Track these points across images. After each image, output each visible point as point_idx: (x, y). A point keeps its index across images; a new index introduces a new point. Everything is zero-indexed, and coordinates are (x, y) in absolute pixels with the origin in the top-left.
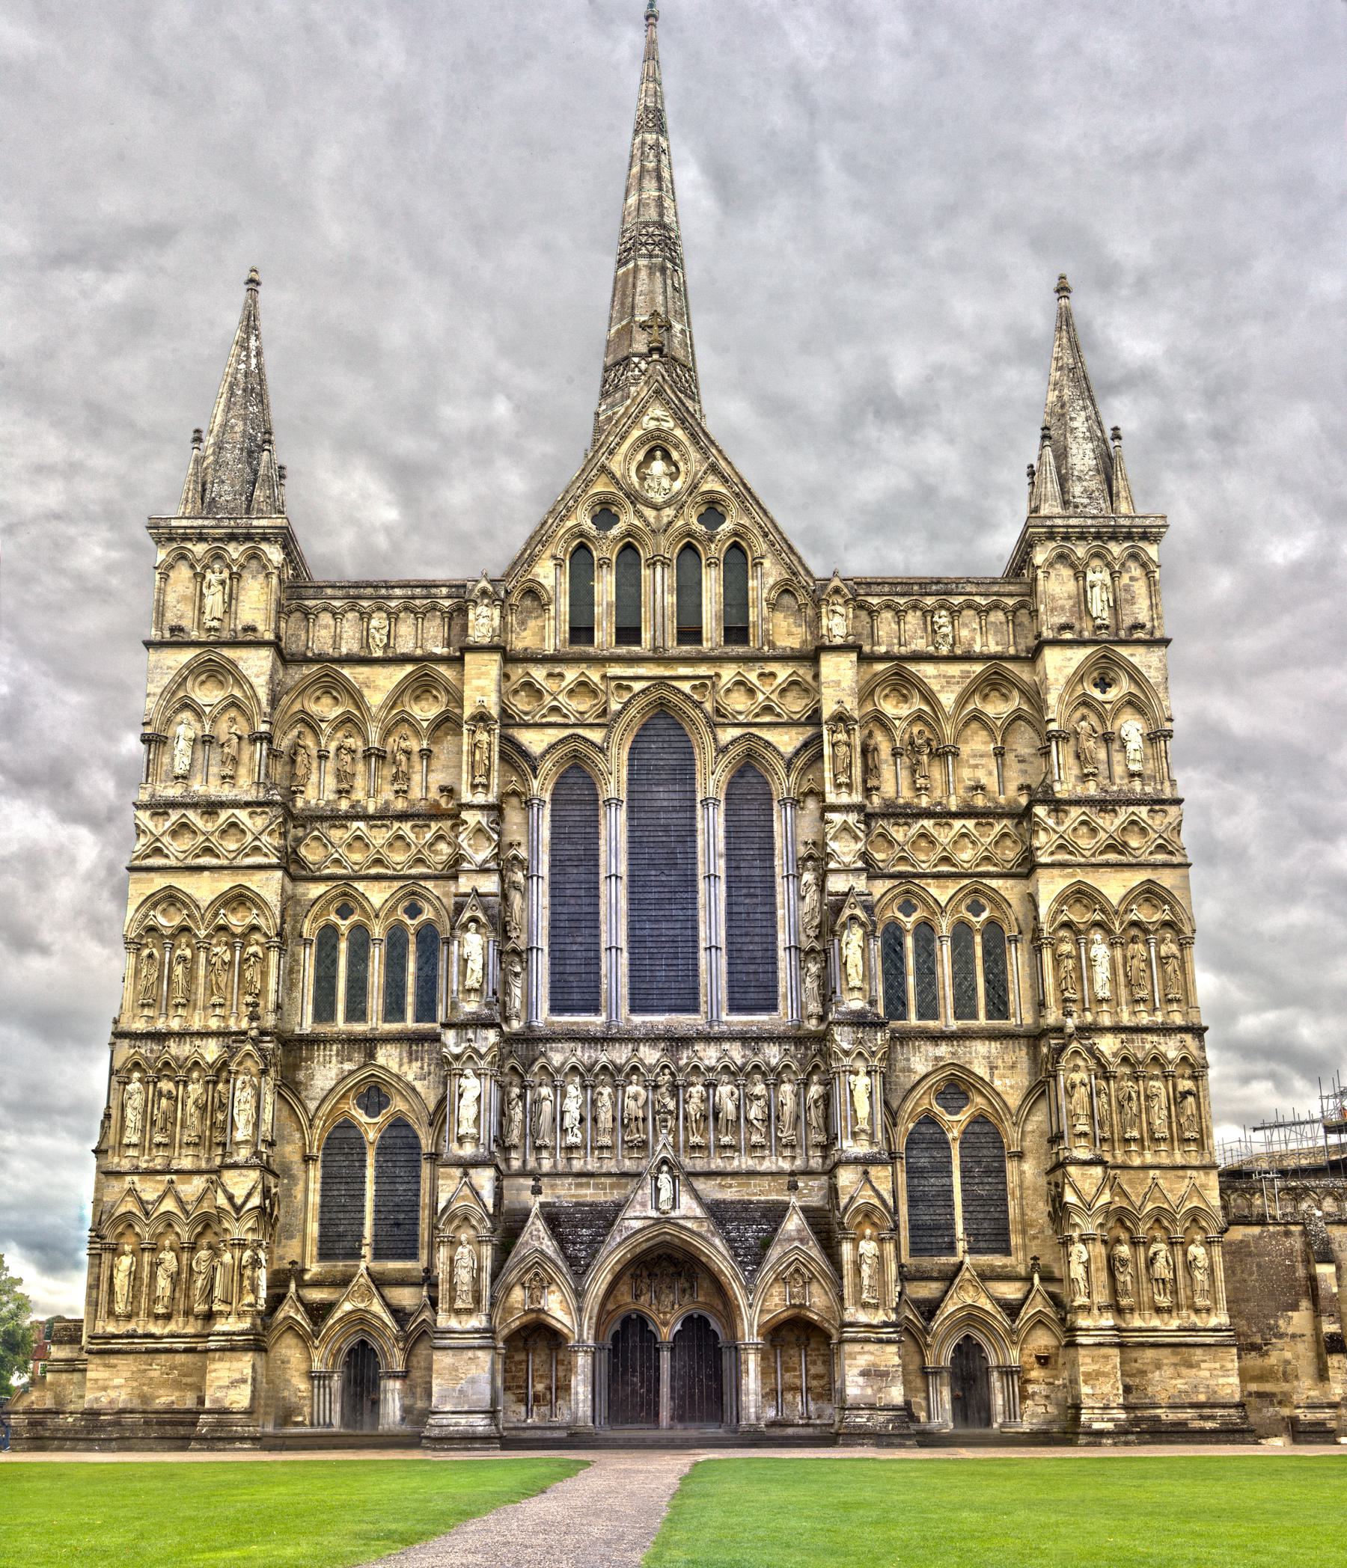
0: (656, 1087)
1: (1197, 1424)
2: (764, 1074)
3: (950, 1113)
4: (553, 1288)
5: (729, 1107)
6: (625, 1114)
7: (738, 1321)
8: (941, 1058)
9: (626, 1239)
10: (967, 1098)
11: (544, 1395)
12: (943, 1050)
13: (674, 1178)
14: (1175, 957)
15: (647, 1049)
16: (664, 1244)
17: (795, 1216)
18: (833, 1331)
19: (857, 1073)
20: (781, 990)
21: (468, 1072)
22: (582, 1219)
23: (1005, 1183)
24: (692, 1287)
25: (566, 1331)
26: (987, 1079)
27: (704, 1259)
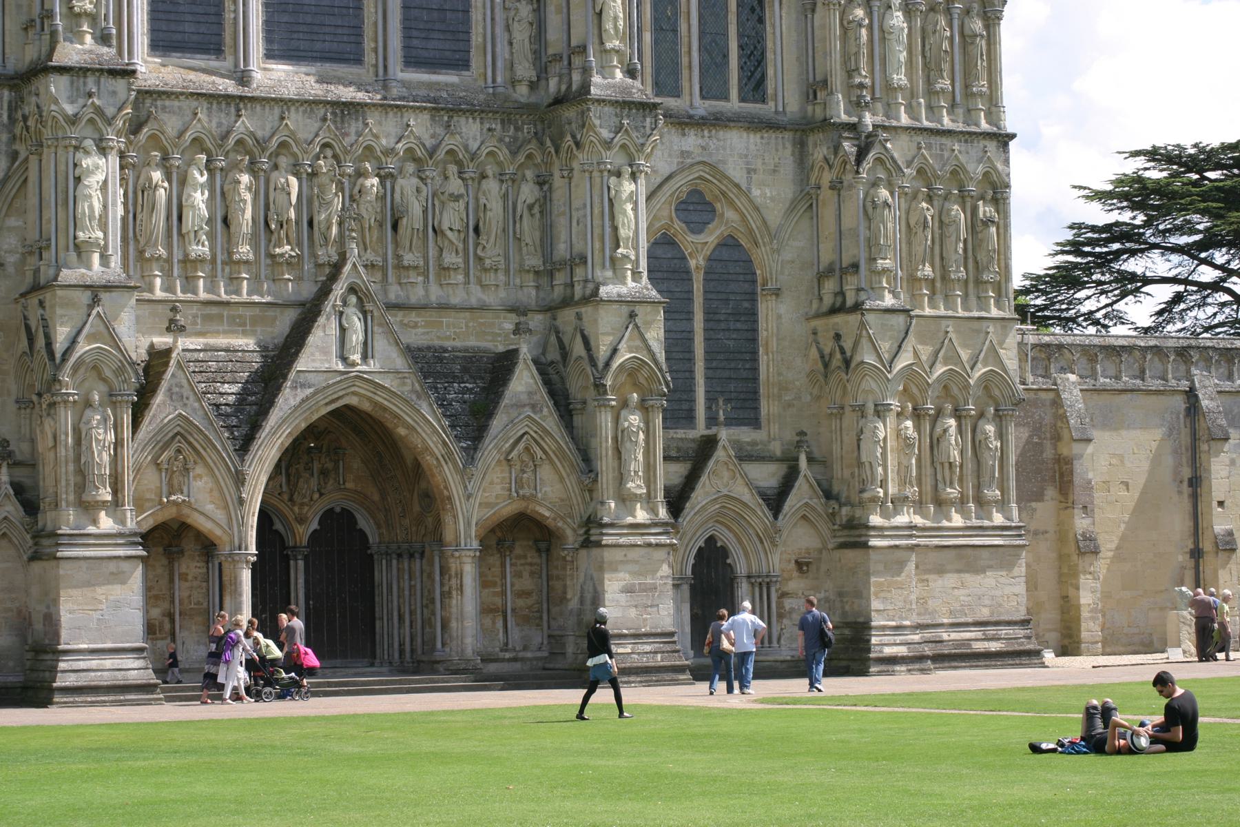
0: (314, 174)
1: (979, 646)
2: (459, 163)
3: (693, 232)
4: (199, 470)
5: (416, 209)
6: (273, 217)
7: (448, 519)
8: (687, 154)
9: (303, 401)
10: (714, 211)
11: (161, 624)
12: (691, 141)
13: (365, 313)
14: (982, 36)
15: (300, 117)
16: (347, 406)
17: (526, 373)
18: (569, 532)
19: (619, 174)
20: (476, 39)
21: (89, 143)
22: (218, 371)
23: (755, 330)
24: (336, 468)
25: (218, 532)
26: (744, 187)
27: (402, 431)
